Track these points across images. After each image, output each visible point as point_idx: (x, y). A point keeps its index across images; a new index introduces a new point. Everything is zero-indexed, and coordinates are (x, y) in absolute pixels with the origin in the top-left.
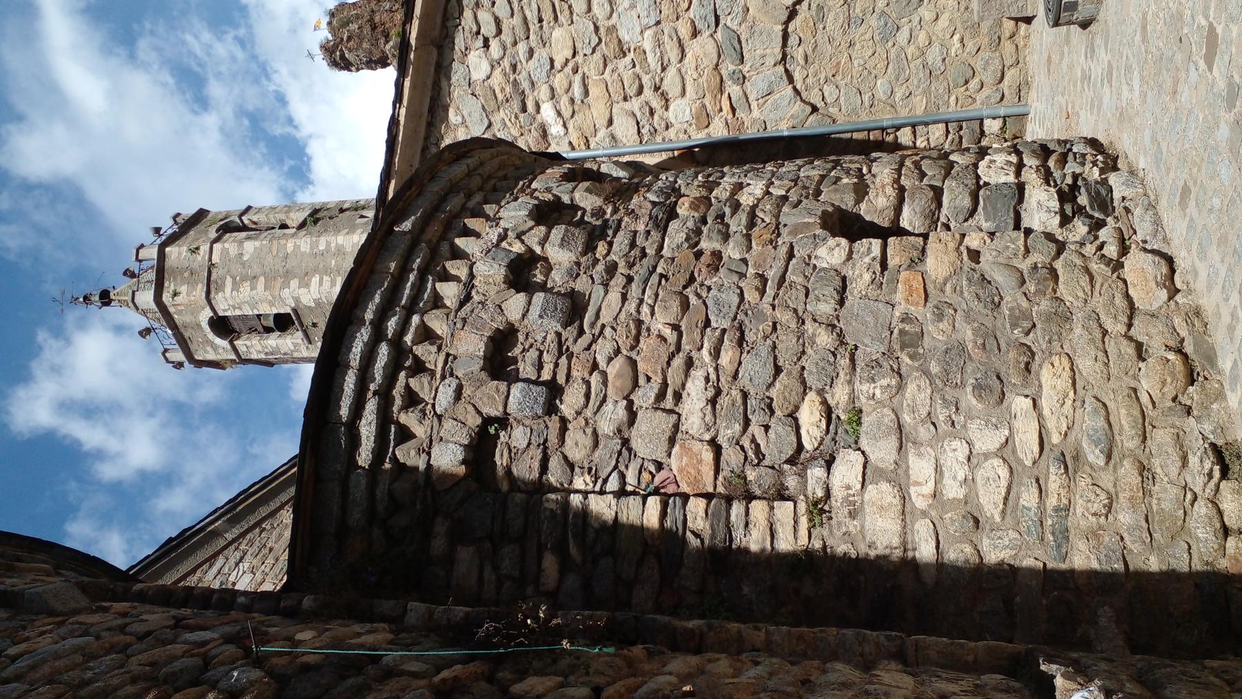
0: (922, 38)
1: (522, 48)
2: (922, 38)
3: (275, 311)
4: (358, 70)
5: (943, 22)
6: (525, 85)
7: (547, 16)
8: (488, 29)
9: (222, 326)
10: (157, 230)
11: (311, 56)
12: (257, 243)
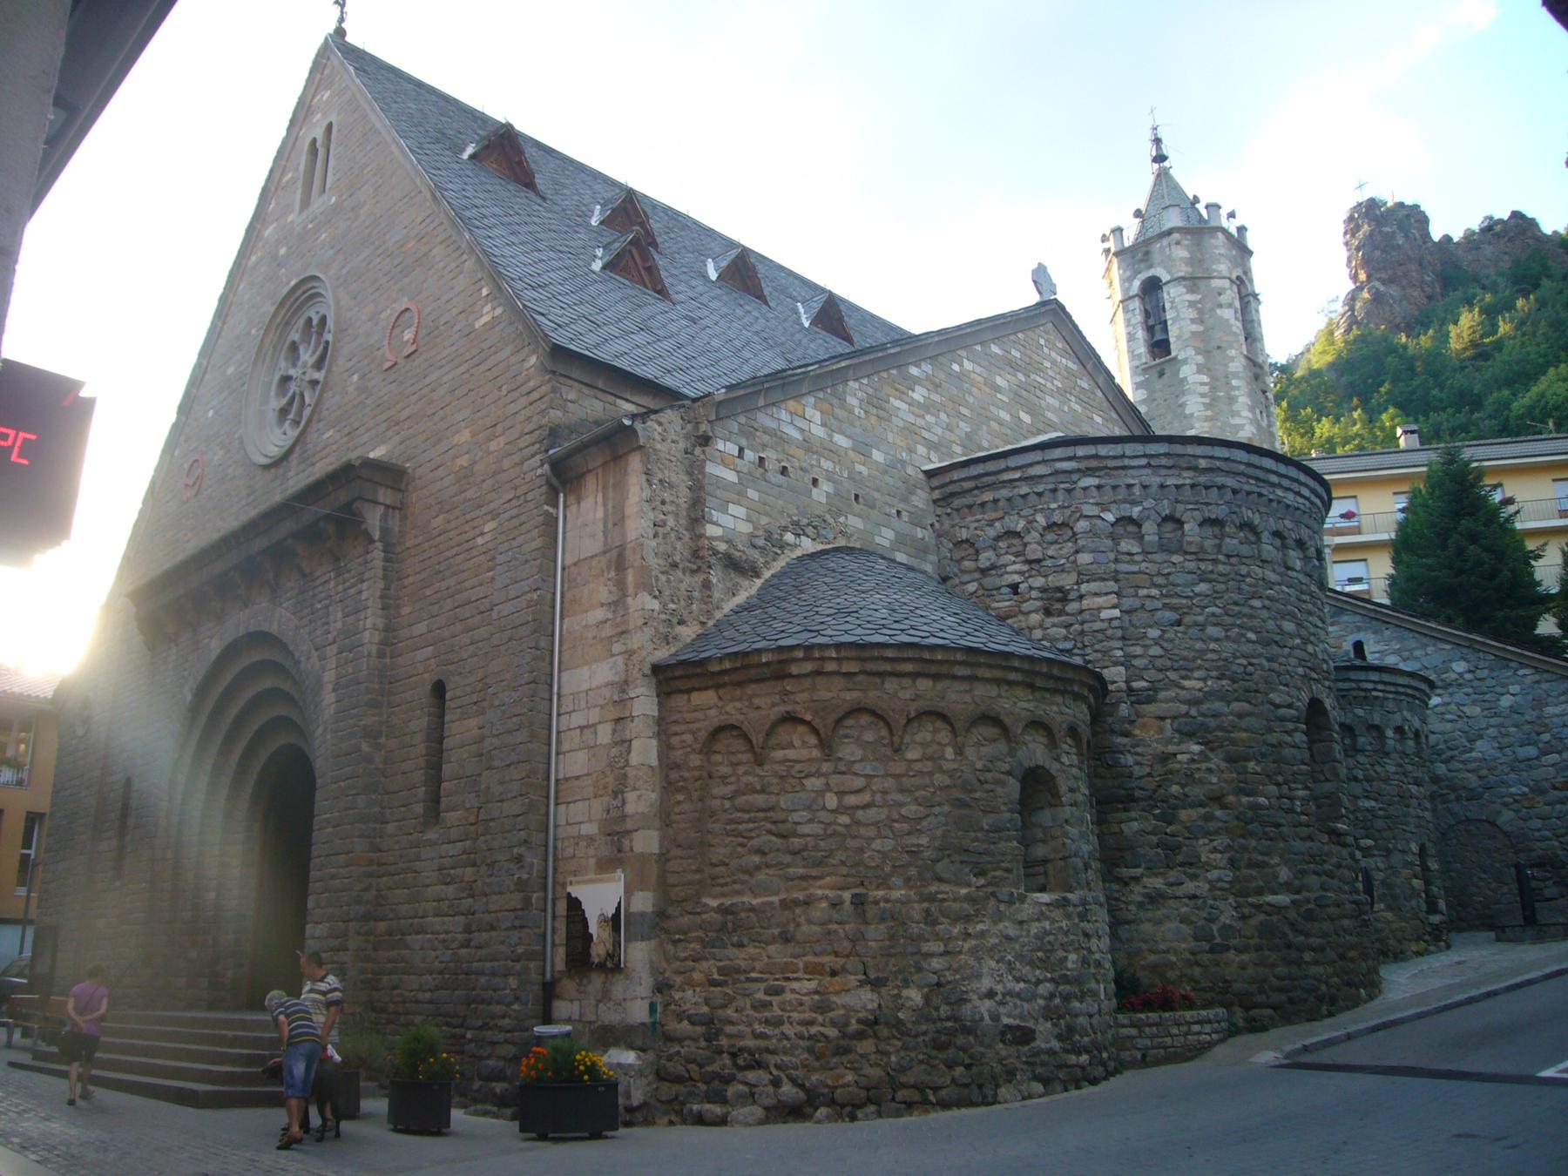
1: (1470, 690)
3: (1172, 340)
4: (1346, 244)
7: (1487, 705)
8: (1479, 674)
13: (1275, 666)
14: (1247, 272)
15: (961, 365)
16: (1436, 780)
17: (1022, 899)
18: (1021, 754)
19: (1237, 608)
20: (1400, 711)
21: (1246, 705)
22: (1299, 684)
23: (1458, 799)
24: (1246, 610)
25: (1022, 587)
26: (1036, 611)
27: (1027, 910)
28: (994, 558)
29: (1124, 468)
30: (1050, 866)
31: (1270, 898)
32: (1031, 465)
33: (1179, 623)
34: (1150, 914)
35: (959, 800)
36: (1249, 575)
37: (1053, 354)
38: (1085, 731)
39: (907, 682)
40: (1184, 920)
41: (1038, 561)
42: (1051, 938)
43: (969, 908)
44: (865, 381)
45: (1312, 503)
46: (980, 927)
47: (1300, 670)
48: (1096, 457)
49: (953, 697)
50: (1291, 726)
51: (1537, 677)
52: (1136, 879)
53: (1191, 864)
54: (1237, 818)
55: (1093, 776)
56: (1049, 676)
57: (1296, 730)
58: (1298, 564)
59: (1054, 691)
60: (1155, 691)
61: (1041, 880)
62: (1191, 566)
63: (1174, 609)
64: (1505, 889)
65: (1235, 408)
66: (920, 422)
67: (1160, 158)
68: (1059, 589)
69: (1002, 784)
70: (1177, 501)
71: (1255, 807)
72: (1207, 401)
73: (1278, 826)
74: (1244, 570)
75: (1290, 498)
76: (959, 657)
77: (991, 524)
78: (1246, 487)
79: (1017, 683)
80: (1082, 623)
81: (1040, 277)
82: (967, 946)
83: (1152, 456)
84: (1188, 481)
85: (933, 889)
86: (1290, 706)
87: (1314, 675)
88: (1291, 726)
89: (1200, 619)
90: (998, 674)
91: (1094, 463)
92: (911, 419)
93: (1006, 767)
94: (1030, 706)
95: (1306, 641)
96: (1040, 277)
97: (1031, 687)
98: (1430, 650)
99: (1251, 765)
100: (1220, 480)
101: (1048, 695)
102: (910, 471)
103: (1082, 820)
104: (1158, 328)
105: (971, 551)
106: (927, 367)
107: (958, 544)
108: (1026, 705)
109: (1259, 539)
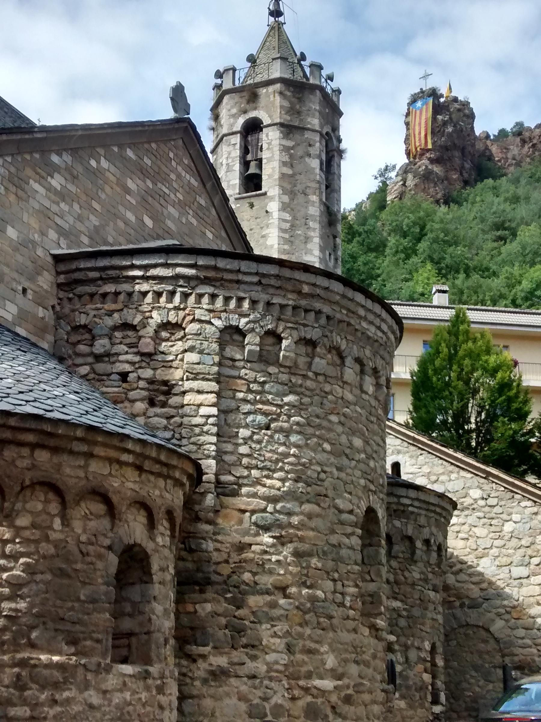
0: (473, 681)
2: (473, 681)
3: (264, 177)
5: (477, 689)
6: (466, 512)
7: (493, 529)
9: (253, 128)
10: (330, 78)
11: (426, 76)
12: (318, 171)
13: (343, 475)
14: (335, 129)
15: (98, 162)
16: (446, 588)
17: (108, 670)
18: (122, 530)
19: (318, 421)
20: (429, 526)
21: (316, 507)
22: (360, 494)
23: (462, 606)
24: (325, 423)
25: (132, 377)
26: (142, 400)
27: (111, 681)
28: (108, 346)
29: (238, 282)
30: (134, 640)
31: (318, 683)
32: (155, 266)
33: (268, 428)
34: (212, 691)
35: (60, 569)
36: (331, 393)
37: (180, 169)
38: (179, 514)
39: (25, 451)
40: (242, 698)
41: (150, 355)
42: (131, 708)
43: (57, 675)
44: (9, 159)
45: (388, 338)
46: (66, 694)
47: (362, 482)
48: (215, 268)
49: (68, 471)
50: (349, 530)
51: (535, 509)
52: (204, 657)
53: (253, 646)
54: (297, 608)
55: (179, 558)
56: (158, 461)
57: (353, 534)
58: (371, 389)
59: (159, 475)
60: (240, 486)
61: (124, 652)
62: (284, 377)
63: (266, 414)
64: (491, 686)
65: (309, 246)
66: (54, 208)
67: (276, 13)
68: (165, 383)
69: (100, 557)
70: (279, 319)
71: (313, 599)
72: (287, 236)
73: (330, 617)
74: (327, 388)
75: (372, 331)
76: (79, 433)
77: (110, 314)
78: (338, 316)
79: (127, 464)
80: (182, 417)
81: (178, 95)
82: (52, 712)
83: (264, 275)
84: (291, 302)
85: (25, 655)
86: (351, 512)
87: (372, 488)
88: (349, 530)
89: (286, 425)
90: (112, 453)
91: (211, 274)
92: (47, 203)
93: (107, 542)
94: (136, 487)
95: (369, 457)
96: (178, 95)
97: (140, 468)
98: (453, 476)
99: (314, 562)
100: (318, 305)
101: (152, 478)
102: (40, 252)
103: (167, 597)
104: (253, 164)
105: (87, 336)
106: (67, 158)
107: (76, 328)
108: (130, 485)
109: (343, 364)
